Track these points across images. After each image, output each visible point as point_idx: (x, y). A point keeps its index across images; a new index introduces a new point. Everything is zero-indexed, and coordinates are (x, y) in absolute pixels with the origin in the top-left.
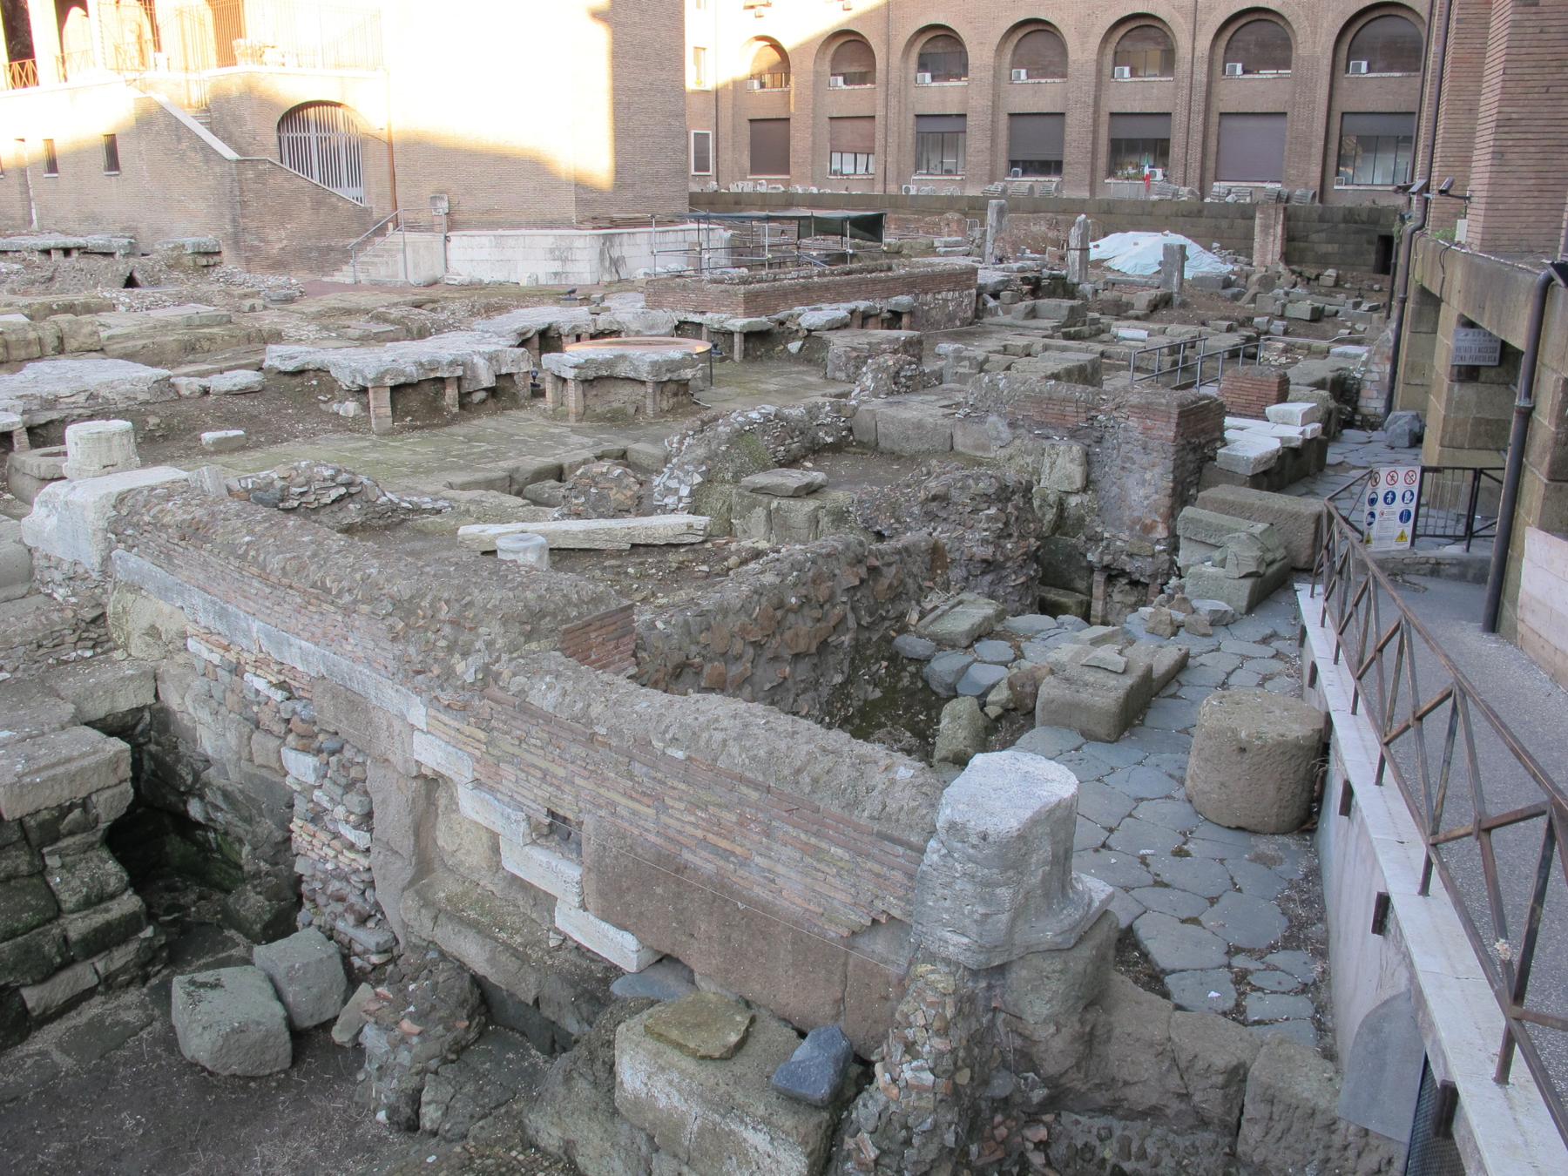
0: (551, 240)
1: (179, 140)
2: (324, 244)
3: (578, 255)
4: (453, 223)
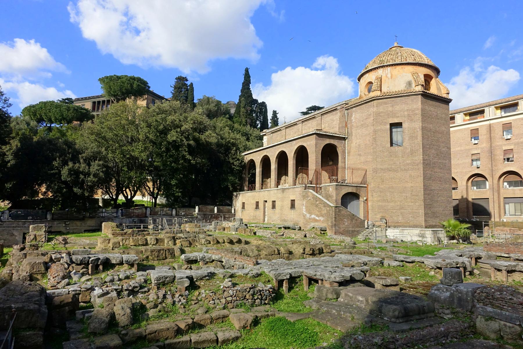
0: (418, 231)
1: (316, 201)
2: (353, 229)
3: (427, 235)
4: (388, 226)
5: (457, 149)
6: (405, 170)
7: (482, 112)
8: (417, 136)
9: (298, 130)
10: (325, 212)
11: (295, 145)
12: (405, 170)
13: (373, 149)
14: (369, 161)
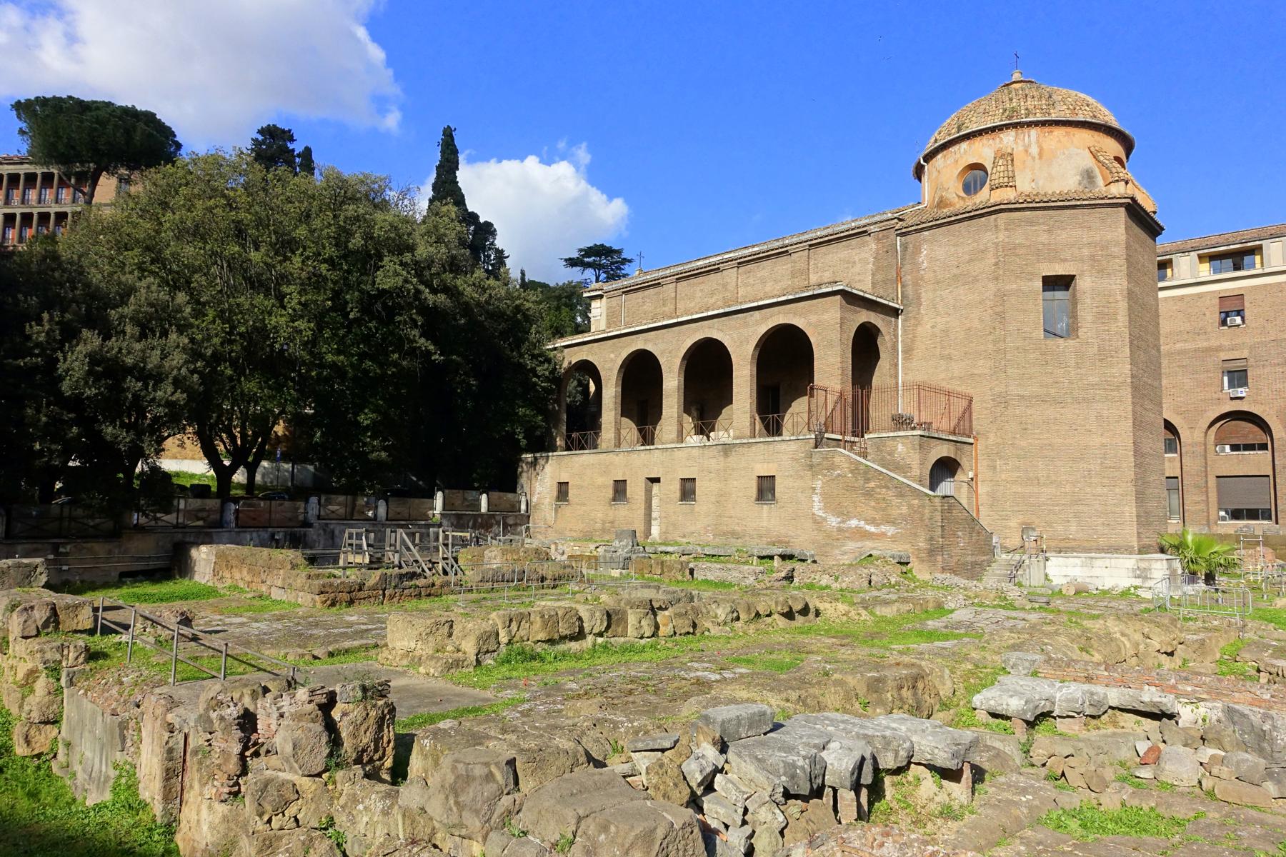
1: (867, 480)
6: (1084, 400)
8: (1116, 313)
10: (905, 510)
11: (757, 323)
12: (1084, 400)
13: (995, 342)
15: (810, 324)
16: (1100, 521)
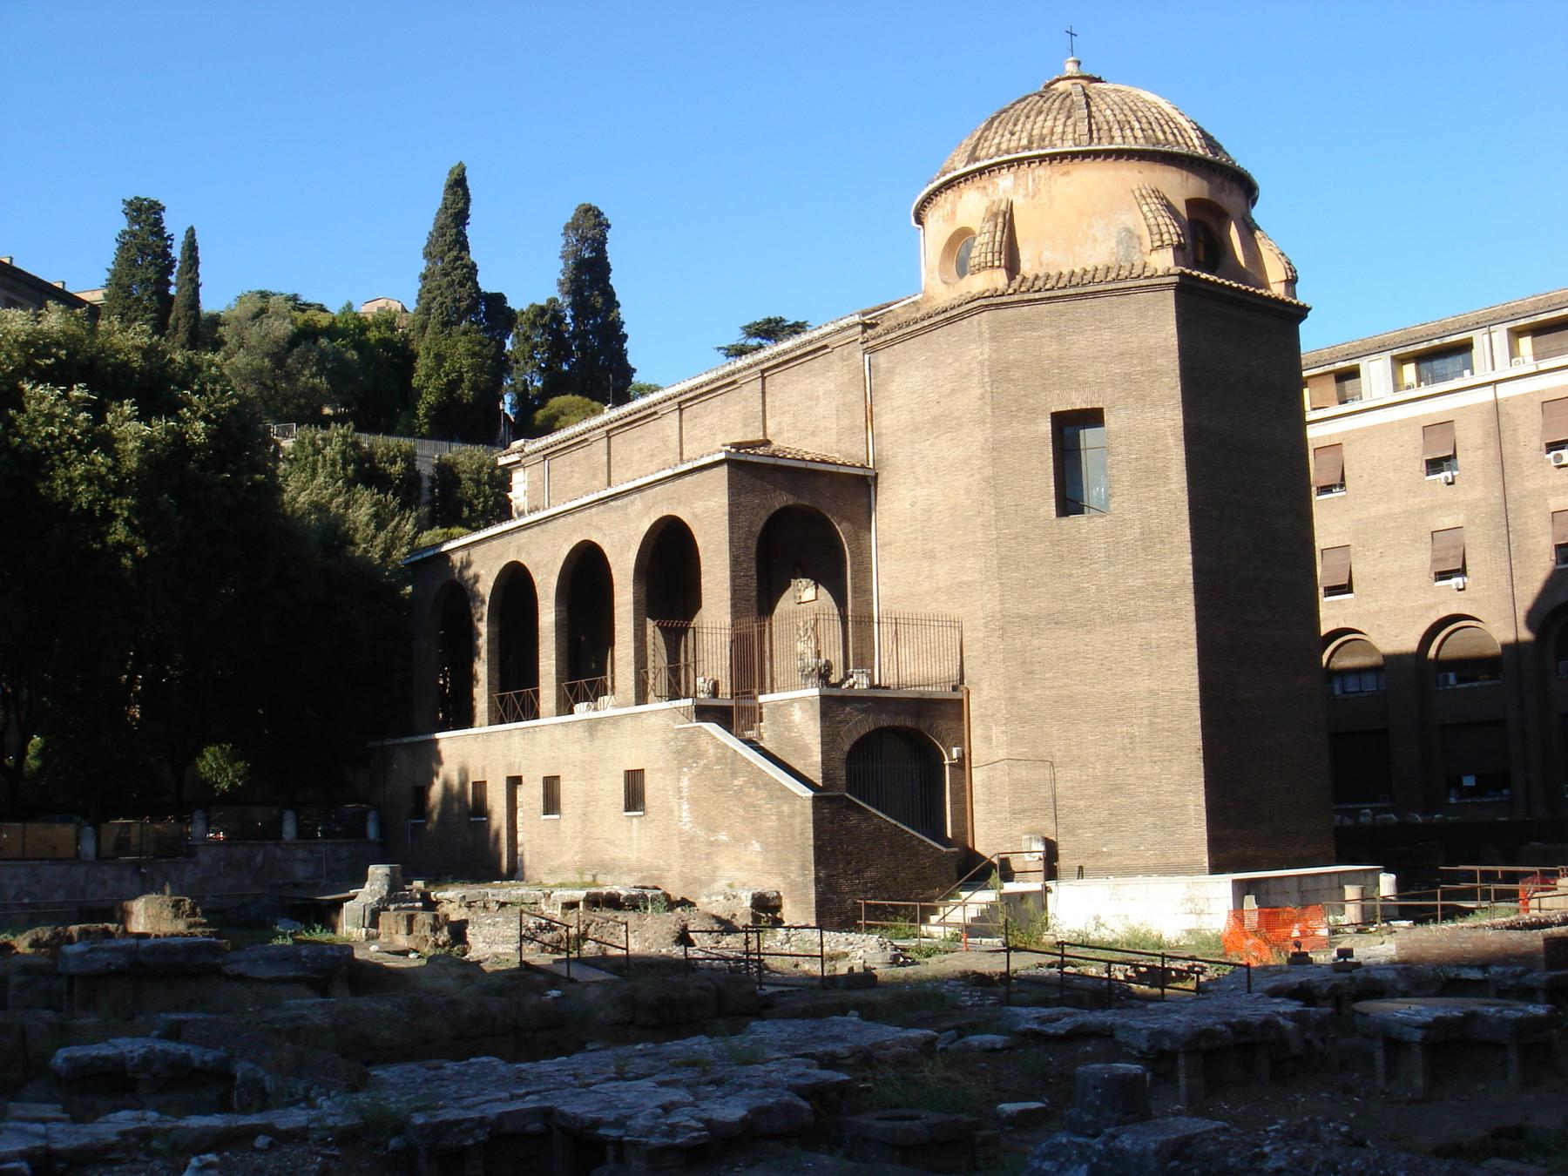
1: (734, 774)
5: (1373, 511)
7: (1465, 347)
9: (665, 441)
12: (1122, 618)
14: (968, 584)
15: (695, 516)
16: (1150, 820)
